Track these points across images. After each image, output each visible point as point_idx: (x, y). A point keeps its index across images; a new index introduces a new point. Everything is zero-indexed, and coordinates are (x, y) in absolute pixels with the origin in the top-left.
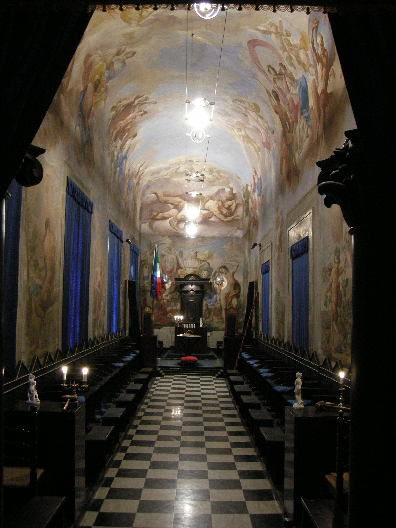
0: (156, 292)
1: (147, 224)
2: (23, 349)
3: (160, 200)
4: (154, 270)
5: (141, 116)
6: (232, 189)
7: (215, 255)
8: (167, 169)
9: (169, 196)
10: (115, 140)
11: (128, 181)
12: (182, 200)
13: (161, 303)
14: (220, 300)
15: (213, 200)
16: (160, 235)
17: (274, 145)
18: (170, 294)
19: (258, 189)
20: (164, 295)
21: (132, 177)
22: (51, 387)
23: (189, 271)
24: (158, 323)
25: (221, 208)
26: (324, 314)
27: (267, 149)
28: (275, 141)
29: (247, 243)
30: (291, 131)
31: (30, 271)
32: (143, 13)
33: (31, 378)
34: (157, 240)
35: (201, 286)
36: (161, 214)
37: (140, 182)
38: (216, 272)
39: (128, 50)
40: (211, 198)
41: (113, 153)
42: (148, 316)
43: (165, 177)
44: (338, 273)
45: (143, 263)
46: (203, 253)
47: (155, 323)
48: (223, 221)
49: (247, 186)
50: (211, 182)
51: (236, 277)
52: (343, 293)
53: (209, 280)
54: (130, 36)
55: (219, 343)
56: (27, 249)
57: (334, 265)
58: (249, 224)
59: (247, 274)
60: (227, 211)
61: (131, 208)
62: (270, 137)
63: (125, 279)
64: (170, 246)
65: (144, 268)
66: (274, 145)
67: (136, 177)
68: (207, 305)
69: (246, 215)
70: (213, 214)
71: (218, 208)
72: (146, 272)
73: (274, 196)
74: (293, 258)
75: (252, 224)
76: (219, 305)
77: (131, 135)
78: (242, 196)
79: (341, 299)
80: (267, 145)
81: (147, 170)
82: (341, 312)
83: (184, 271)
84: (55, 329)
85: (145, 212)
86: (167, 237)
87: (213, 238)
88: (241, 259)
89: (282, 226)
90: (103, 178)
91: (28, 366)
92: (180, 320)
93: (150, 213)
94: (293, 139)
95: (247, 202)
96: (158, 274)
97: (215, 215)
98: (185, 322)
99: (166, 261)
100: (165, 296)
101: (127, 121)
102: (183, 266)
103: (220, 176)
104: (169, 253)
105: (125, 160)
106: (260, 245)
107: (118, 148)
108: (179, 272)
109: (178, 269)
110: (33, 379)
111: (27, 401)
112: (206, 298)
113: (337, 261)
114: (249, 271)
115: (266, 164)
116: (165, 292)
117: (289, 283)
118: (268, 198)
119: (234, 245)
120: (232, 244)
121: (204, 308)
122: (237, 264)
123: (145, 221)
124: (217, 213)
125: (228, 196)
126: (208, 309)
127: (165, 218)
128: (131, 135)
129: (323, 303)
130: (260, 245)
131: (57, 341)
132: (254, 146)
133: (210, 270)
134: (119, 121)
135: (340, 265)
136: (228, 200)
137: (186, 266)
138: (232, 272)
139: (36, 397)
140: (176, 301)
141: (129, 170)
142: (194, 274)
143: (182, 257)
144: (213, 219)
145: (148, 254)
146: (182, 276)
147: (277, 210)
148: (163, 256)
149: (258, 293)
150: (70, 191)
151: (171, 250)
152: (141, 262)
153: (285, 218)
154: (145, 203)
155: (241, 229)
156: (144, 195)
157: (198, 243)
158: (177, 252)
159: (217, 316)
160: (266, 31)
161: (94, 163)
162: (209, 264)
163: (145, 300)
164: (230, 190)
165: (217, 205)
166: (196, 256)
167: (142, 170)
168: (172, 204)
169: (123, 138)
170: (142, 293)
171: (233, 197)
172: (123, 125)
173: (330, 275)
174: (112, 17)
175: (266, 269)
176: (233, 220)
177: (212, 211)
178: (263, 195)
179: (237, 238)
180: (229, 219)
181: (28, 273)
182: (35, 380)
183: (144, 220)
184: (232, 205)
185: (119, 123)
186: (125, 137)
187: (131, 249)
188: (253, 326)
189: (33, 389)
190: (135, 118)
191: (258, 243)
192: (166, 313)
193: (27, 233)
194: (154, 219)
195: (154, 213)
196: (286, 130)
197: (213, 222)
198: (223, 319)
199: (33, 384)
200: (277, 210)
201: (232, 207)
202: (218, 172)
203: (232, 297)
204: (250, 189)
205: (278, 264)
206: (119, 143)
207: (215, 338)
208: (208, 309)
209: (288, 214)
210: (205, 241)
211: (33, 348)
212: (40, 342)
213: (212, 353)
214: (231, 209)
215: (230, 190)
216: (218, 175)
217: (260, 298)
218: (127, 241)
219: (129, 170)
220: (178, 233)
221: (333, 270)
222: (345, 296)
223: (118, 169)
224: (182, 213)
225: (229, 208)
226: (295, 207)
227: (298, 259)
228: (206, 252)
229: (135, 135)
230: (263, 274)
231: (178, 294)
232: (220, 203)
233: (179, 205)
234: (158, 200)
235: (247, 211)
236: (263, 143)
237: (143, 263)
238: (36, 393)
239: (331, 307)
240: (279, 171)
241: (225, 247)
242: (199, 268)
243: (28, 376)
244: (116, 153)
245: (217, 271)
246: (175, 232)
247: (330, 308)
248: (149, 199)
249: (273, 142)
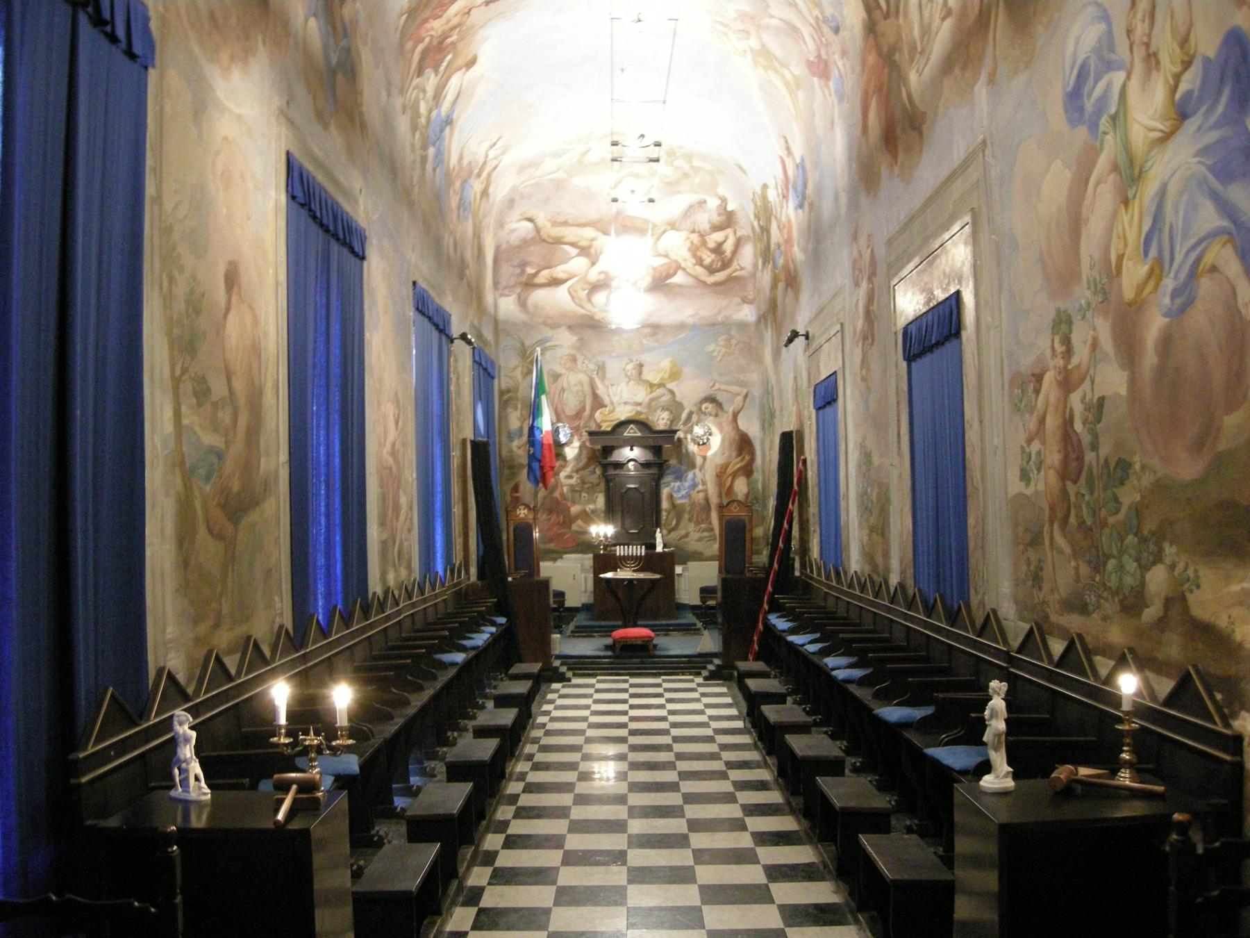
0: (542, 468)
1: (514, 297)
2: (171, 631)
3: (544, 236)
4: (534, 411)
5: (483, 7)
6: (724, 201)
7: (688, 371)
8: (557, 155)
9: (565, 224)
10: (420, 72)
11: (458, 185)
13: (557, 495)
14: (704, 483)
15: (678, 230)
16: (545, 324)
17: (840, 64)
18: (577, 471)
19: (795, 189)
20: (562, 474)
21: (470, 174)
22: (242, 752)
23: (623, 413)
24: (551, 546)
25: (697, 249)
26: (1019, 502)
27: (820, 77)
28: (844, 53)
29: (768, 335)
30: (893, 9)
31: (184, 409)
33: (181, 724)
34: (539, 338)
35: (657, 450)
37: (491, 190)
38: (690, 414)
40: (673, 226)
41: (416, 107)
42: (523, 532)
43: (553, 176)
44: (1067, 384)
45: (505, 397)
46: (658, 365)
47: (542, 546)
48: (704, 283)
49: (765, 187)
50: (670, 184)
51: (742, 424)
52: (1086, 439)
53: (675, 432)
55: (706, 592)
56: (171, 348)
57: (1051, 364)
58: (774, 287)
59: (772, 415)
60: (713, 256)
61: (469, 255)
62: (827, 45)
63: (461, 437)
64: (573, 352)
65: (509, 410)
66: (840, 64)
67: (479, 175)
68: (671, 497)
69: (764, 263)
70: (679, 267)
71: (689, 250)
72: (515, 420)
73: (843, 200)
74: (910, 358)
75: (781, 285)
76: (701, 495)
77: (461, 61)
78: (752, 217)
79: (1080, 458)
80: (820, 68)
81: (506, 160)
82: (1080, 495)
83: (610, 412)
84: (270, 571)
85: (507, 270)
86: (564, 328)
87: (682, 326)
88: (754, 377)
89: (872, 275)
90: (392, 168)
91: (189, 681)
92: (605, 536)
93: (518, 271)
94: (899, 37)
95: (765, 230)
96: (546, 423)
97: (684, 269)
98: (619, 540)
99: (563, 390)
100: (565, 477)
101: (449, 21)
102: (607, 400)
103: (692, 167)
104: (570, 370)
105: (447, 130)
106: (807, 336)
107: (430, 94)
108: (598, 415)
109: (594, 410)
110: (186, 727)
111: (173, 793)
112: (668, 479)
113: (1060, 349)
114: (777, 405)
115: (820, 122)
116: (563, 467)
117: (899, 426)
118: (827, 207)
119: (734, 342)
120: (728, 340)
121: (665, 504)
122: (745, 391)
123: (506, 292)
124: (689, 263)
125: (716, 219)
126: (674, 506)
127: (556, 282)
128: (461, 61)
129: (1014, 475)
130: (807, 336)
131: (278, 605)
132: (782, 76)
133: (675, 407)
134: (426, 21)
136: (716, 228)
137: (615, 400)
138: (731, 410)
139: (197, 779)
140: (592, 489)
141: (461, 158)
142: (637, 418)
143: (603, 378)
144: (679, 278)
145: (518, 374)
146: (606, 427)
147: (855, 238)
148: (556, 377)
149: (805, 462)
150: (299, 193)
151: (574, 360)
152: (502, 393)
153: (881, 252)
154: (504, 246)
155: (751, 302)
156: (501, 224)
158: (592, 366)
159: (698, 523)
161: (363, 126)
162: (672, 392)
163: (516, 489)
164: (719, 202)
166: (640, 374)
167: (494, 158)
168: (572, 244)
169: (442, 68)
170: (506, 472)
171: (728, 220)
172: (439, 32)
173: (1037, 391)
175: (826, 396)
176: (730, 280)
177: (674, 258)
178: (811, 204)
179: (742, 326)
180: (720, 276)
181: (177, 415)
182: (191, 728)
183: (506, 287)
185: (427, 25)
186: (445, 64)
187: (475, 361)
188: (795, 544)
189: (188, 755)
190: (468, 13)
191: (802, 332)
192: (569, 521)
193: (168, 300)
194: (530, 284)
195: (530, 270)
196: (877, 15)
197: (680, 286)
198: (712, 530)
199: (187, 740)
200: (855, 238)
202: (689, 157)
203: (734, 475)
204: (772, 195)
205: (864, 379)
206: (431, 80)
207: (696, 578)
208: (674, 506)
209: (889, 242)
210: (659, 337)
211: (203, 628)
212: (225, 611)
213: (690, 618)
214: (723, 253)
217: (812, 474)
218: (463, 337)
219: (461, 158)
220: (591, 318)
221: (1049, 378)
222: (1094, 447)
223: (431, 151)
224: (599, 267)
225: (718, 250)
226: (912, 219)
227: (927, 359)
228: (666, 364)
229: (472, 63)
230: (818, 409)
231: (598, 471)
232: (695, 237)
233: (590, 247)
234: (538, 238)
235: (766, 255)
236: (810, 64)
237: (505, 397)
238: (196, 768)
239: (1045, 482)
240: (858, 131)
241: (711, 347)
242: (649, 406)
243: (172, 716)
244: (423, 108)
245: (694, 409)
246: (584, 316)
247: (1041, 487)
248: (516, 234)
249: (837, 57)
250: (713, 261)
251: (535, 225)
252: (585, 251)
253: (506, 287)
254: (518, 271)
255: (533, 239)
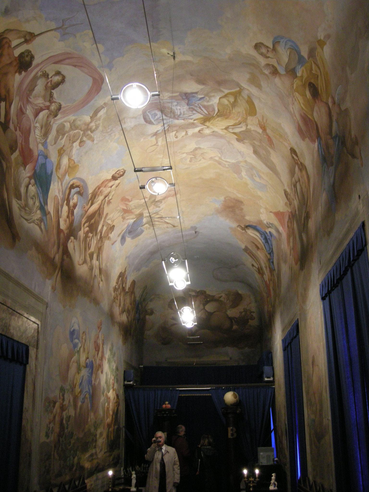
32: (233, 100)
39: (263, 61)
44: (63, 408)
52: (66, 426)
54: (254, 81)
57: (59, 401)
79: (64, 430)
82: (63, 441)
113: (61, 397)
129: (43, 434)
135: (65, 403)
160: (96, 115)
173: (54, 407)
174: (265, 121)
221: (57, 405)
222: (67, 428)
239: (52, 437)
247: (52, 439)
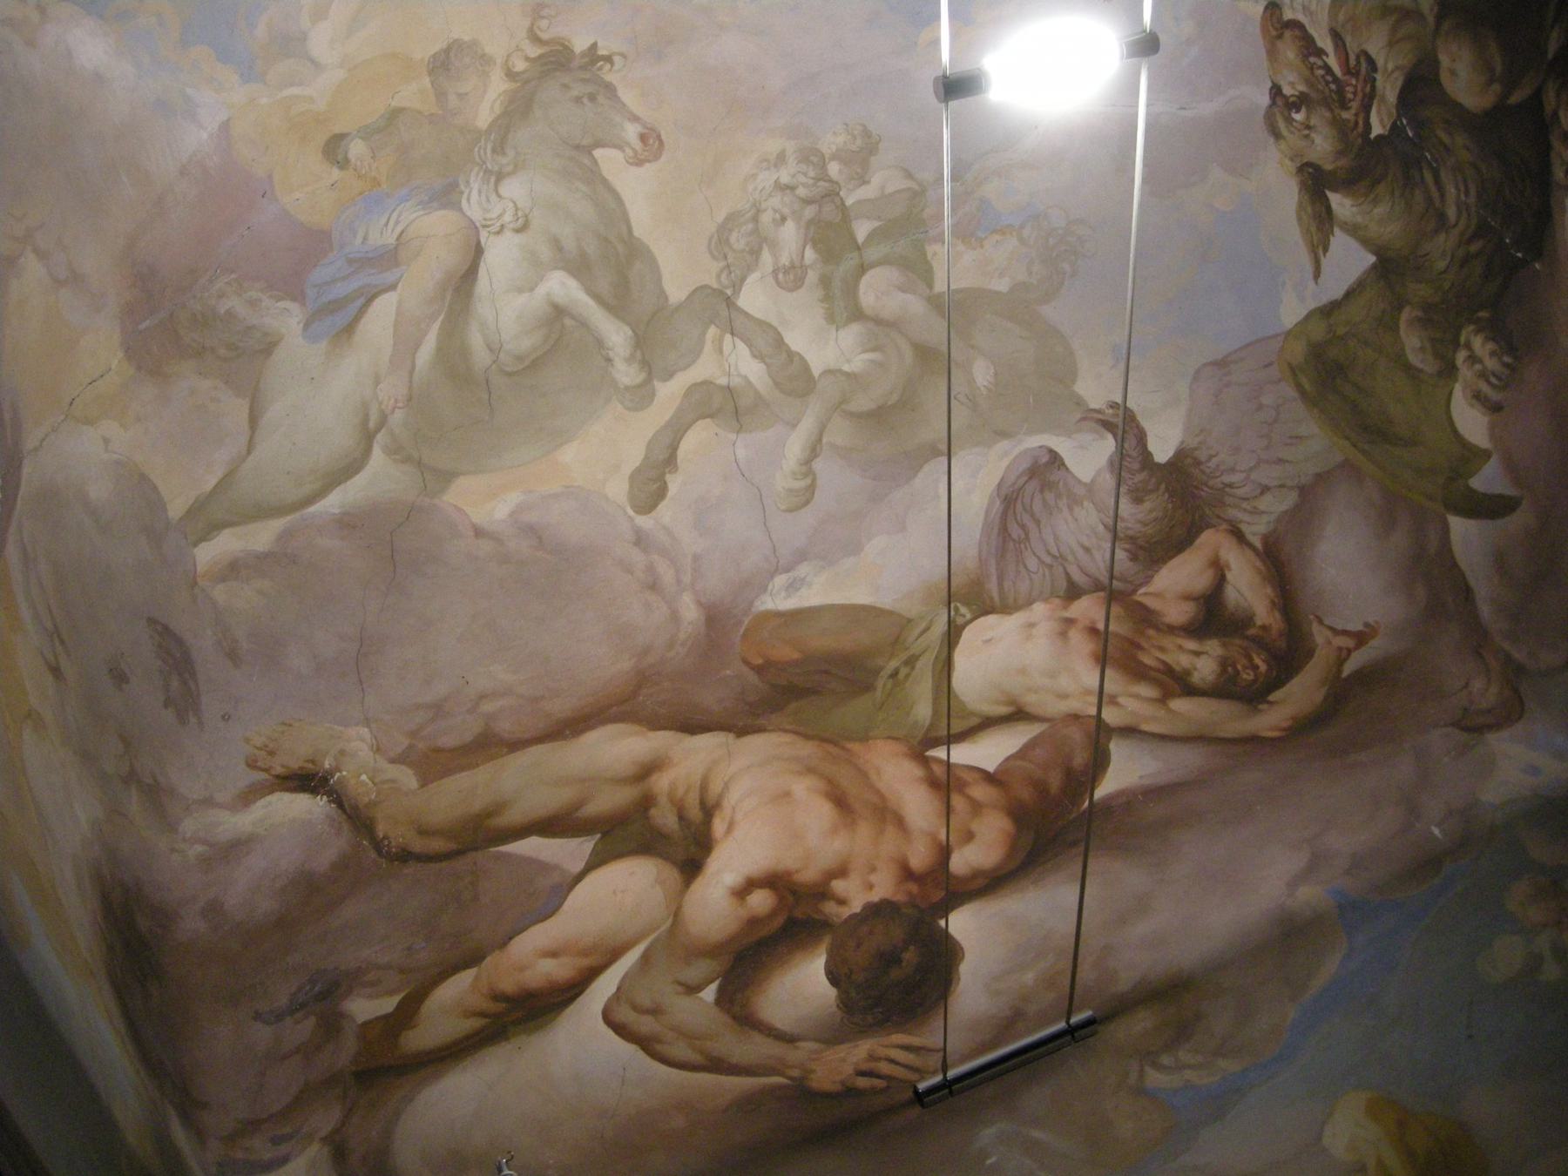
6: (1123, 426)
9: (489, 745)
12: (660, 740)
15: (1006, 609)
36: (465, 978)
48: (1253, 740)
50: (879, 418)
60: (1214, 647)
70: (1099, 735)
87: (1290, 937)
93: (302, 1029)
124: (1133, 702)
127: (535, 1008)
144: (1126, 770)
157: (1155, 1078)
165: (1076, 636)
168: (552, 826)
171: (1181, 500)
176: (1343, 693)
180: (1300, 694)
183: (253, 1126)
184: (1221, 581)
194: (388, 1066)
201: (1231, 595)
215: (1108, 444)
216: (913, 305)
225: (1212, 615)
232: (1088, 608)
233: (646, 803)
246: (748, 1104)
250: (1224, 663)
251: (338, 798)
252: (627, 830)
253: (253, 1126)
254: (302, 1029)
255: (342, 865)
